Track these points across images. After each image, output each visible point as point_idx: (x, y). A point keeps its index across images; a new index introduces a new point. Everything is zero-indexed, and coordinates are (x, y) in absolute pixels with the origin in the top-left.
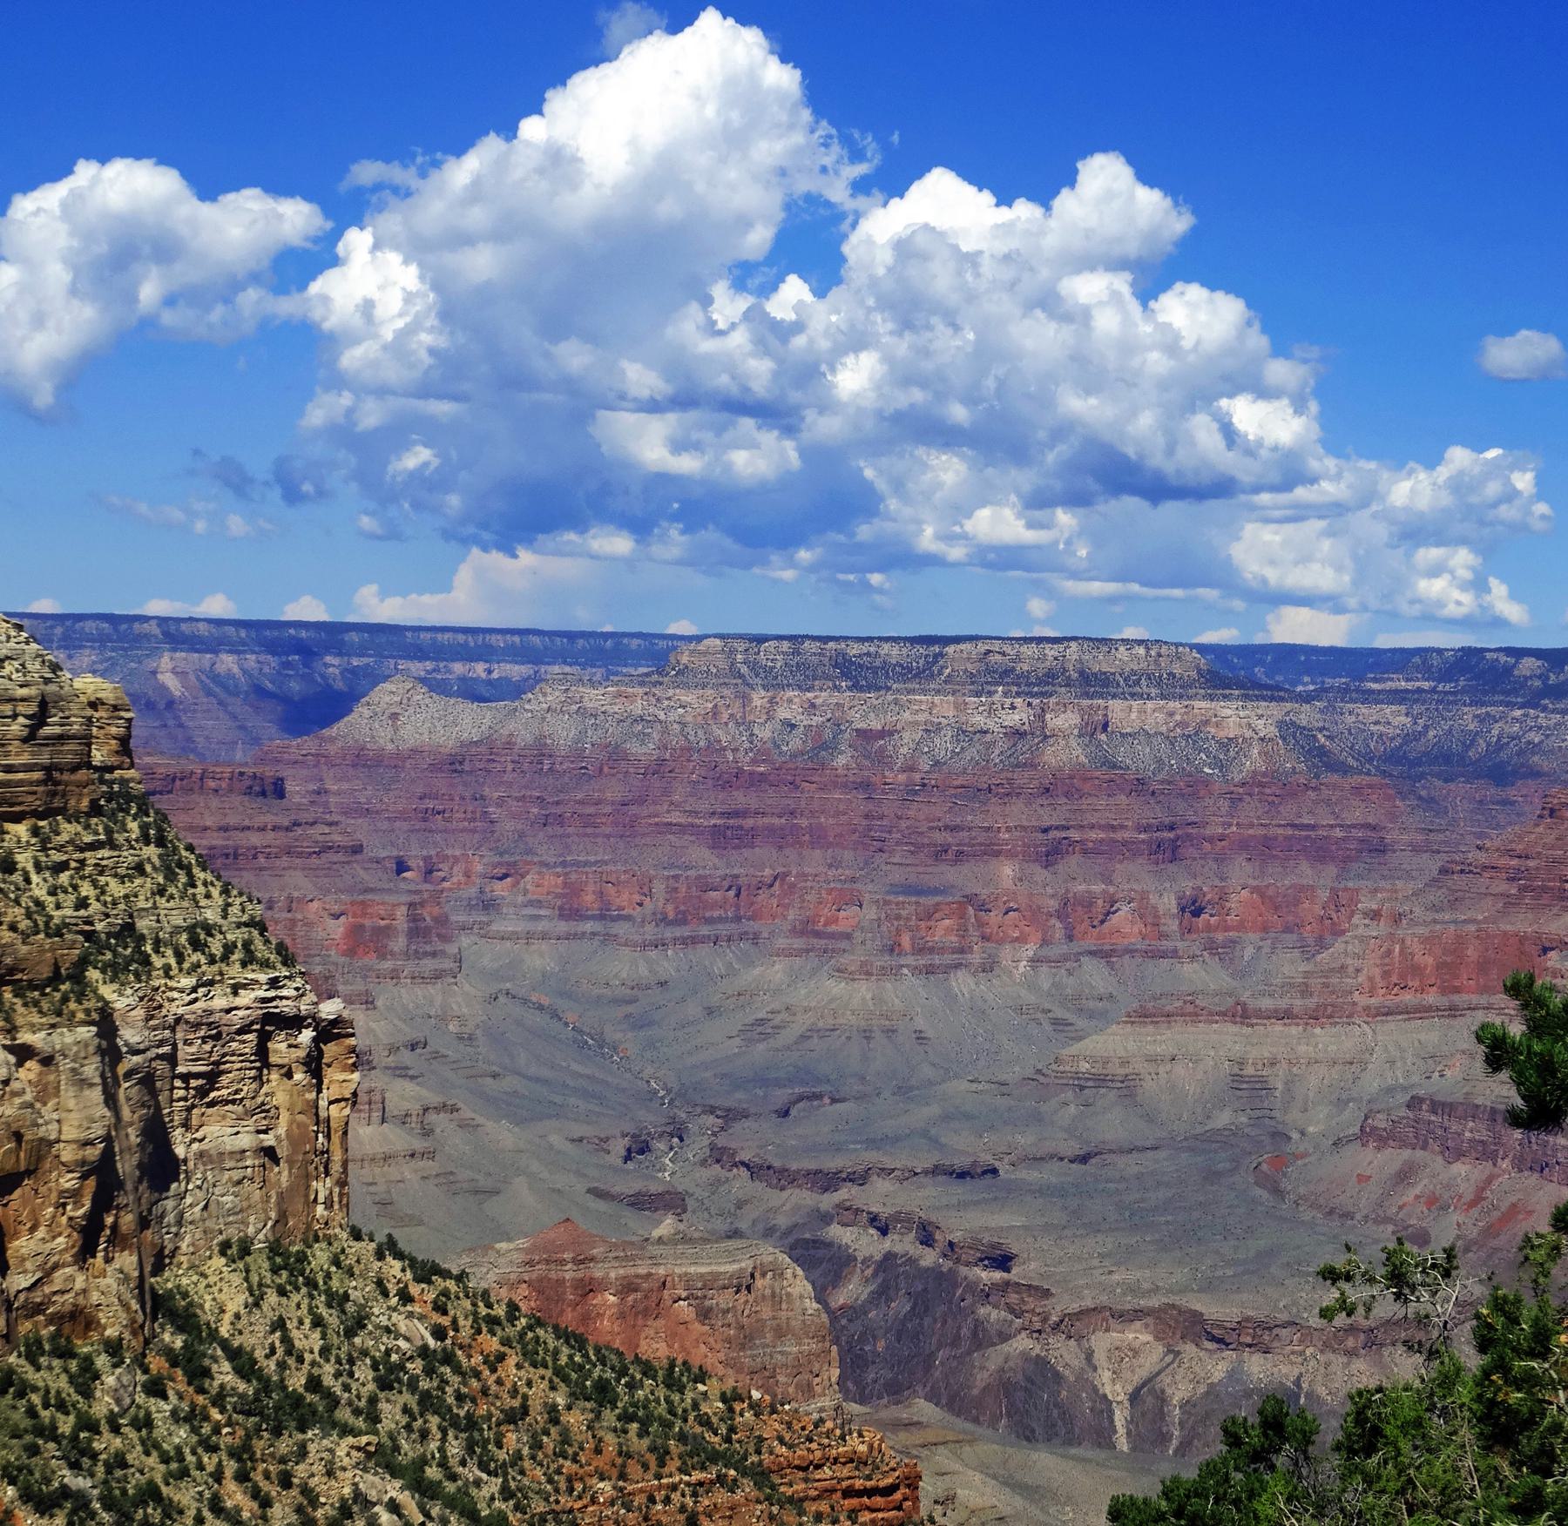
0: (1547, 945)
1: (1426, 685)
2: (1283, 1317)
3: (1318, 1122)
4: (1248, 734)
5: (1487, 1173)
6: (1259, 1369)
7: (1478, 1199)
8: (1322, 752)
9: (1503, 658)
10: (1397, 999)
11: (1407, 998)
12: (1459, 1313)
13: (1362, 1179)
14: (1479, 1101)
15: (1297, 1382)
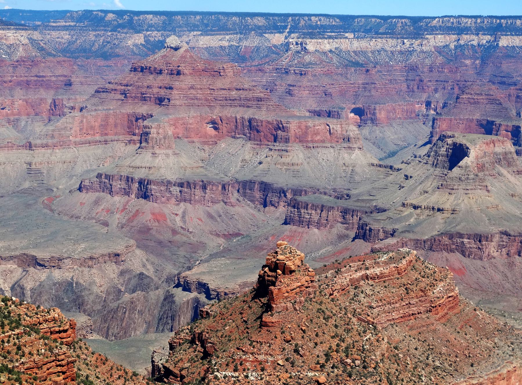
0: (138, 117)
1: (72, 24)
2: (66, 255)
3: (63, 184)
4: (18, 42)
5: (127, 199)
6: (57, 275)
7: (124, 209)
8: (42, 49)
9: (100, 14)
10: (86, 138)
11: (89, 138)
12: (127, 250)
13: (81, 204)
14: (122, 174)
15: (72, 279)
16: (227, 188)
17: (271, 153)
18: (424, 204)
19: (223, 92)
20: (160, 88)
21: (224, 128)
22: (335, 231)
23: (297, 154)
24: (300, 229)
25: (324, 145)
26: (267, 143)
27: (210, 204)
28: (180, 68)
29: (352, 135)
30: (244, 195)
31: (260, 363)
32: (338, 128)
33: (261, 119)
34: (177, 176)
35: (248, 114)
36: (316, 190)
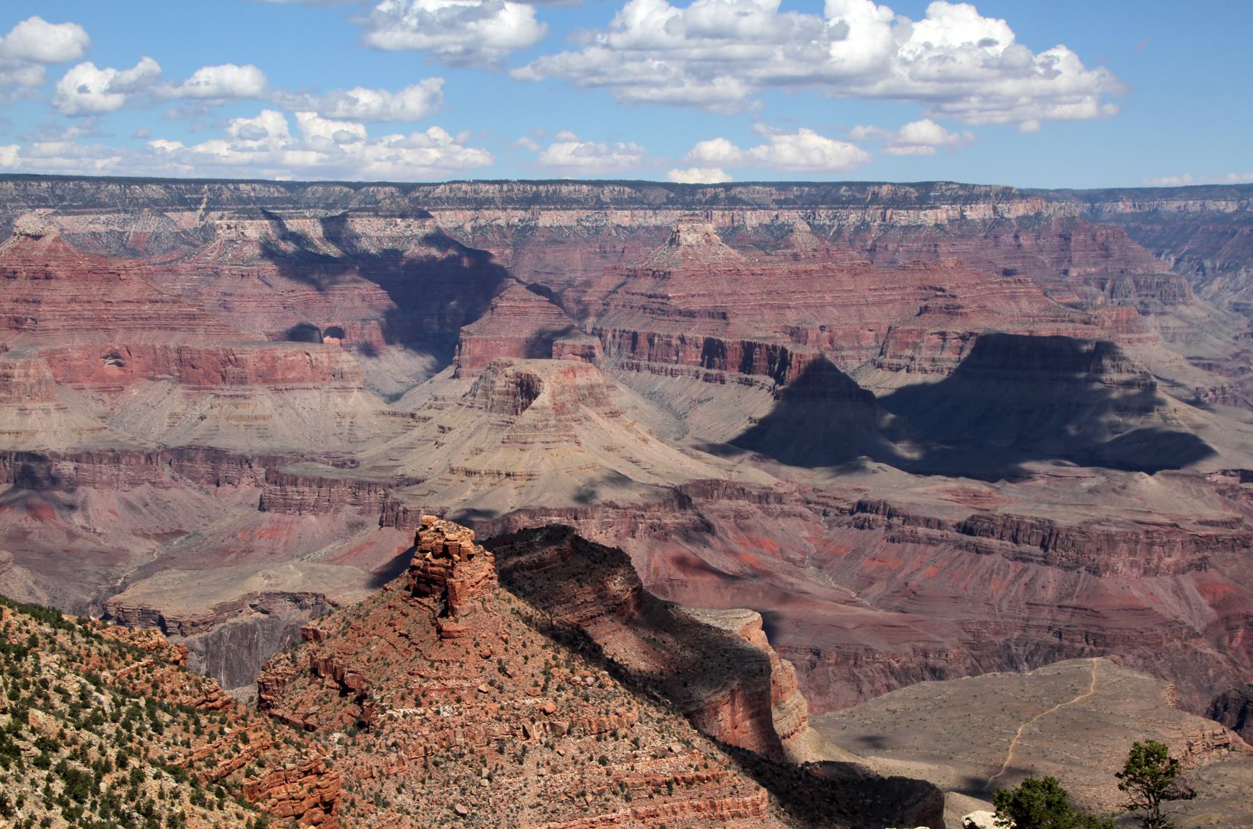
16: (154, 460)
17: (219, 401)
18: (483, 468)
19: (128, 306)
20: (17, 301)
21: (134, 364)
22: (342, 517)
23: (262, 401)
24: (287, 518)
25: (303, 385)
26: (210, 385)
27: (127, 487)
28: (49, 268)
29: (346, 367)
30: (180, 470)
31: (453, 691)
32: (323, 357)
33: (197, 347)
34: (68, 444)
35: (175, 340)
36: (298, 457)
